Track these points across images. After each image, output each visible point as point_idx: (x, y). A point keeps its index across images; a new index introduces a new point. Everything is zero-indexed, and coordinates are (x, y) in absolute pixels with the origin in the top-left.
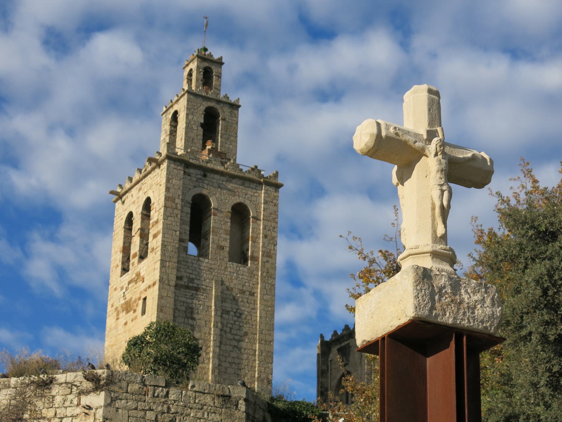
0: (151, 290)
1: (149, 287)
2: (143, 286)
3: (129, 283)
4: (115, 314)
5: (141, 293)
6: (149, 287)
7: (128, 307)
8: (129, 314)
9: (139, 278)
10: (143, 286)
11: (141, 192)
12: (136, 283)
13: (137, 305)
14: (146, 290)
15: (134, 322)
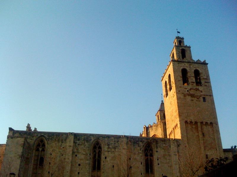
0: (208, 97)
1: (207, 95)
2: (202, 93)
3: (191, 89)
4: (183, 95)
5: (201, 95)
6: (207, 95)
7: (192, 96)
8: (193, 98)
9: (197, 90)
10: (202, 93)
11: (191, 66)
12: (197, 91)
13: (199, 98)
14: (205, 95)
15: (198, 102)
